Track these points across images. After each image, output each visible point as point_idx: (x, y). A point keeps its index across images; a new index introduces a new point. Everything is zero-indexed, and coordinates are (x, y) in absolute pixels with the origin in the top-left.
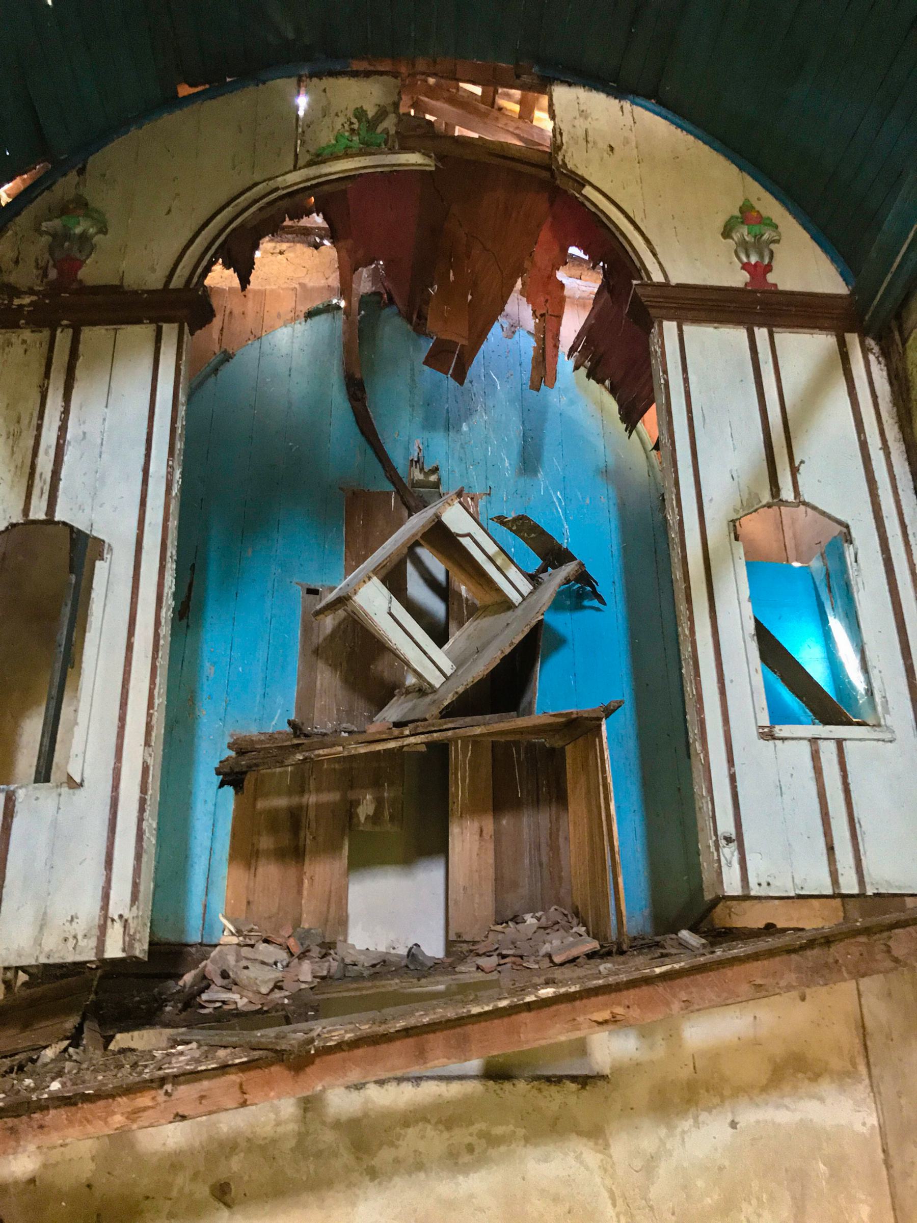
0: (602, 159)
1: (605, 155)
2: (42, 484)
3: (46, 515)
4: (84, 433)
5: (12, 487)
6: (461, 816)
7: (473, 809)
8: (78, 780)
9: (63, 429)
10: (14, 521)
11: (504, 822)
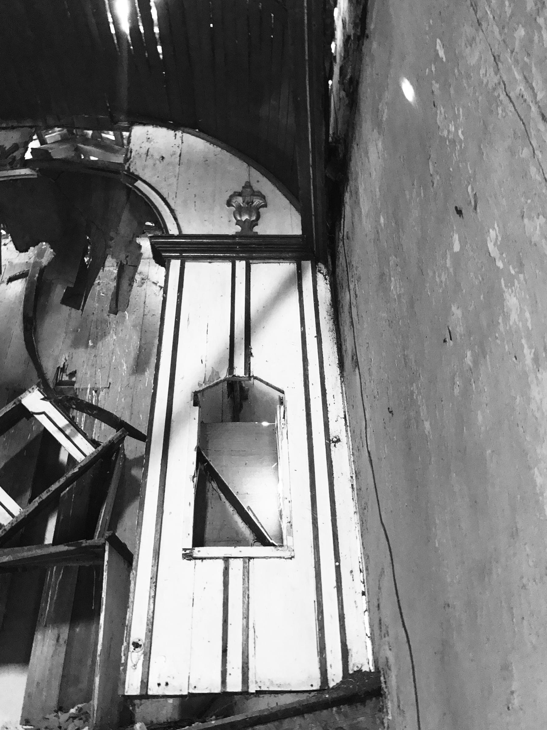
0: (154, 165)
1: (158, 162)
6: (46, 626)
7: (56, 620)
11: (78, 630)
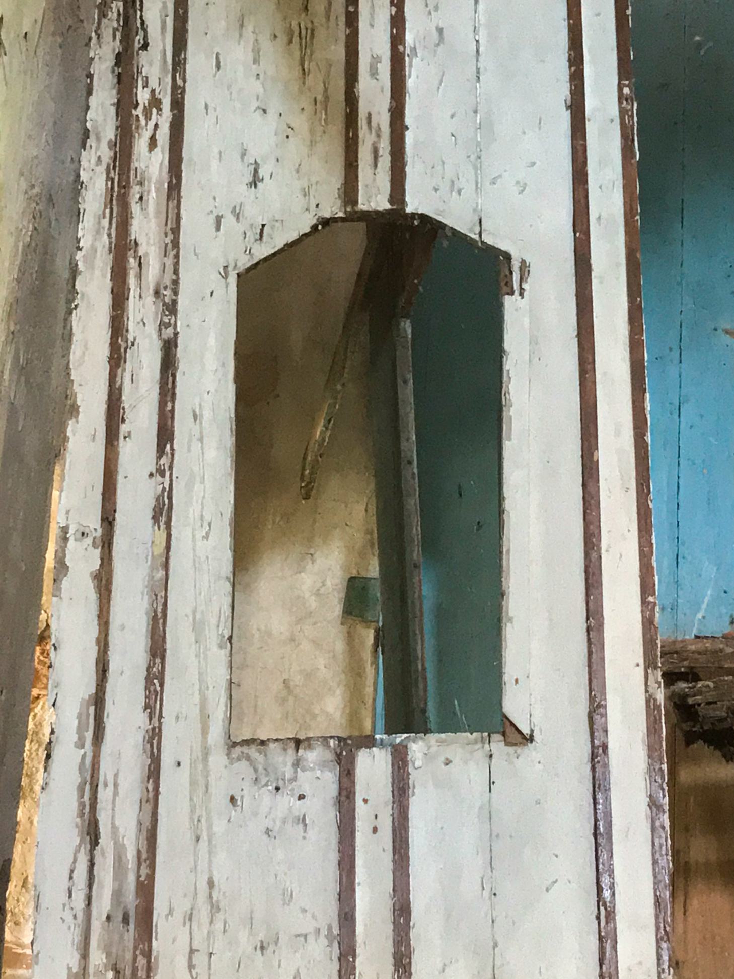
2: (373, 138)
3: (391, 201)
4: (440, 31)
5: (312, 143)
8: (526, 731)
9: (398, 22)
10: (327, 215)
